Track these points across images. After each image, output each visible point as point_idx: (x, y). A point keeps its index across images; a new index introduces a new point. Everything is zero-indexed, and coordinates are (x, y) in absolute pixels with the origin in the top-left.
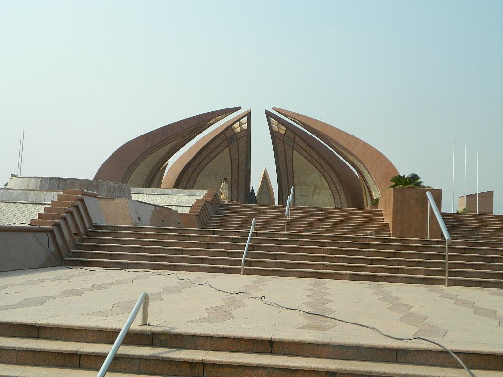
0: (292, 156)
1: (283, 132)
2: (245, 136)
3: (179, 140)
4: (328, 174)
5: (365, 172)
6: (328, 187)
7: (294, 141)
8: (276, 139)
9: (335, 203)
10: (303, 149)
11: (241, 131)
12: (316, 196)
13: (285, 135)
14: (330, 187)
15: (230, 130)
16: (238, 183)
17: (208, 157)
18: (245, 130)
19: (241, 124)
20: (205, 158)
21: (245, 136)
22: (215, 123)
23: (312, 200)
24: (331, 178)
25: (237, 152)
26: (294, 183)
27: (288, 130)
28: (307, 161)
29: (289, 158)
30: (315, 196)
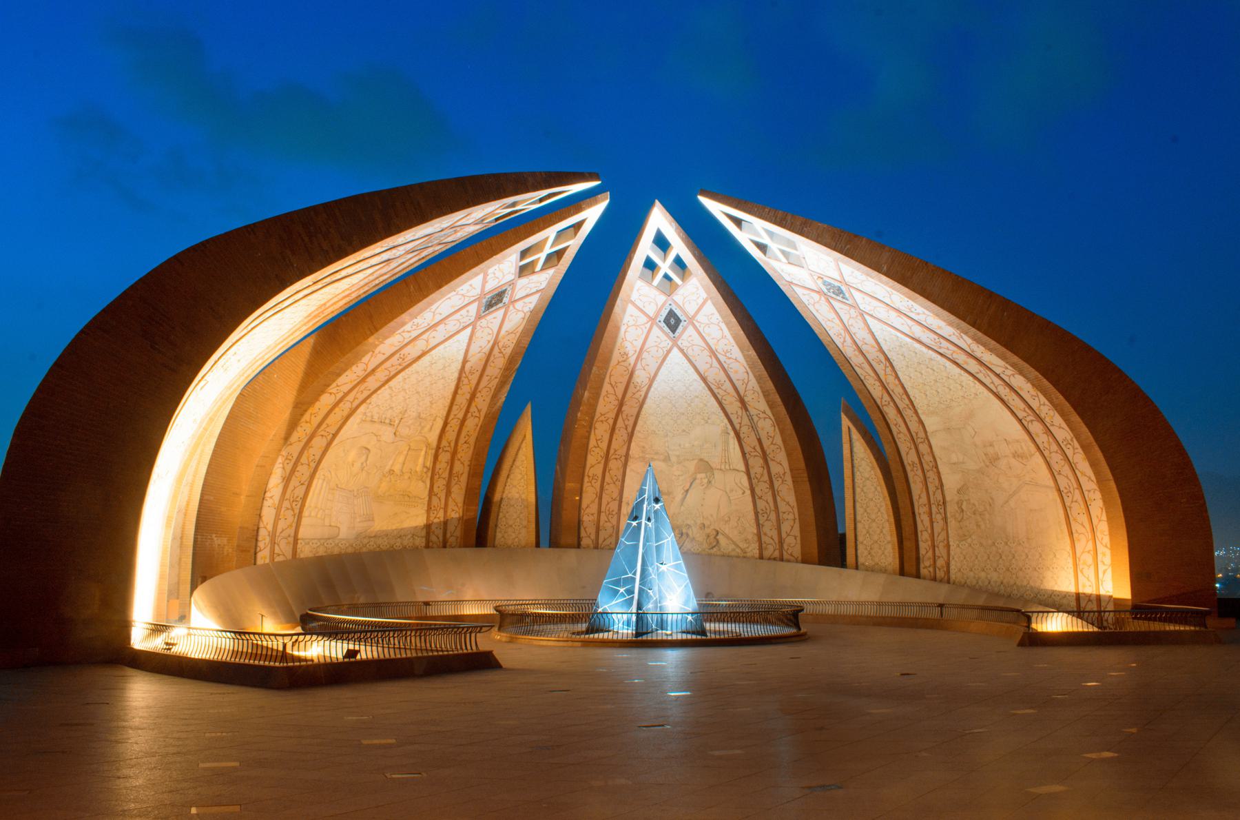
6: (742, 467)
7: (691, 320)
9: (756, 513)
14: (747, 465)
16: (454, 453)
24: (759, 440)
26: (627, 456)
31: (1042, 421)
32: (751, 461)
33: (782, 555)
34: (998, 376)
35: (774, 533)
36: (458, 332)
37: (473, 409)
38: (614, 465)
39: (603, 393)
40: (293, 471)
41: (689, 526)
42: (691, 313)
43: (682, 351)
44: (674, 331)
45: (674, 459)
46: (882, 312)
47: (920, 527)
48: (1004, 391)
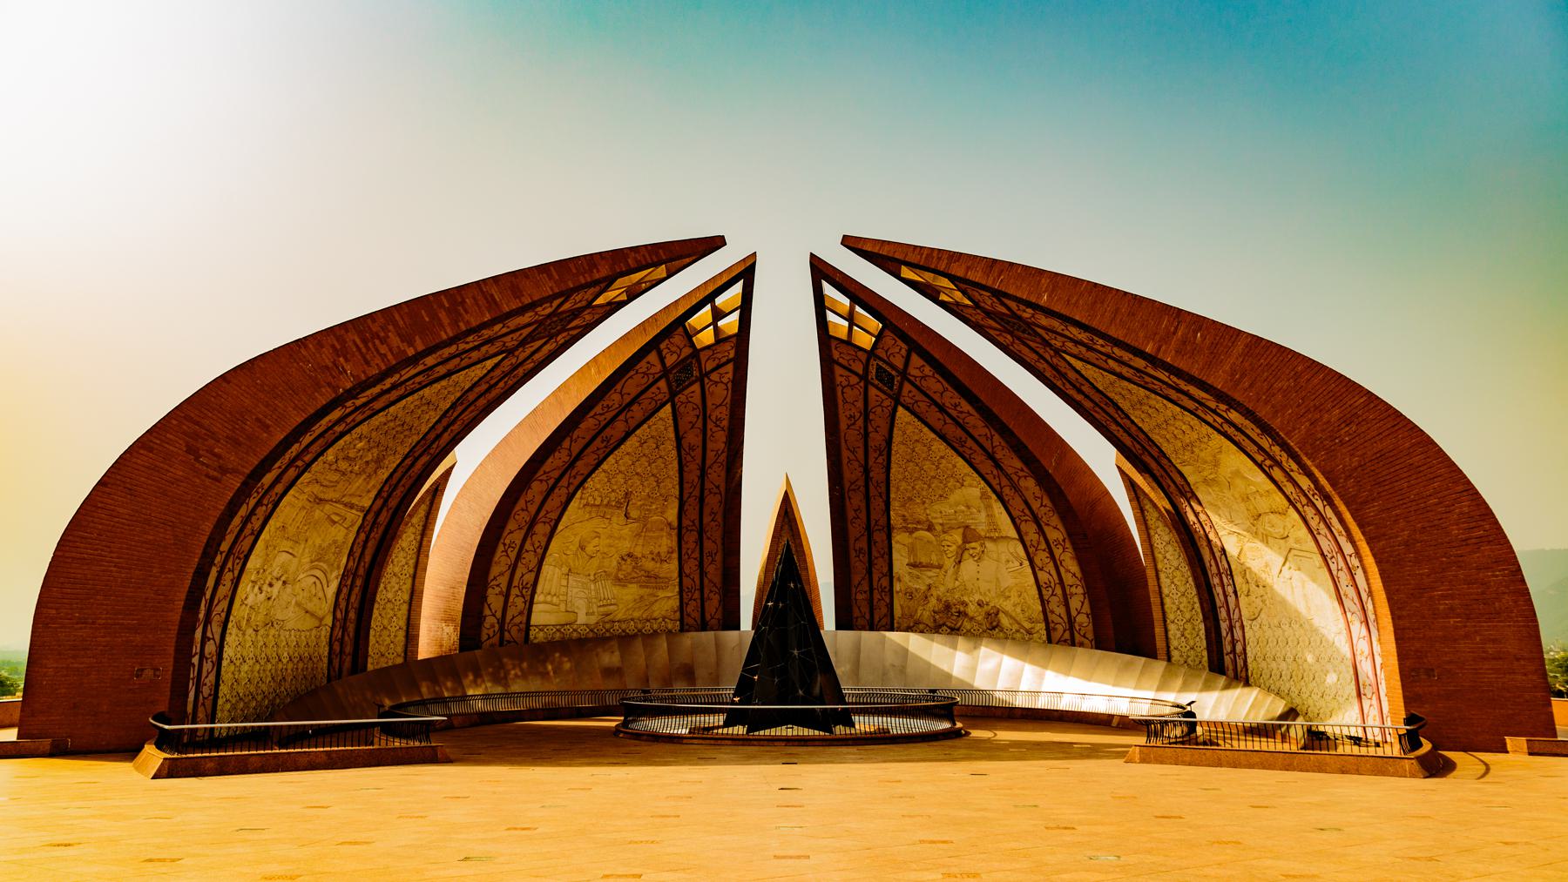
3: (489, 364)
4: (1016, 488)
6: (1014, 534)
7: (904, 374)
8: (838, 371)
10: (937, 405)
12: (969, 566)
13: (872, 353)
15: (678, 339)
16: (701, 532)
17: (598, 440)
19: (718, 314)
20: (587, 445)
24: (1026, 502)
25: (699, 424)
27: (887, 333)
28: (943, 446)
29: (876, 439)
31: (1279, 464)
32: (1023, 527)
33: (1072, 635)
34: (1214, 411)
35: (1061, 610)
36: (657, 410)
37: (708, 485)
38: (879, 537)
39: (845, 461)
41: (965, 604)
43: (907, 408)
44: (891, 388)
45: (939, 528)
46: (1075, 350)
47: (1218, 604)
48: (1231, 431)
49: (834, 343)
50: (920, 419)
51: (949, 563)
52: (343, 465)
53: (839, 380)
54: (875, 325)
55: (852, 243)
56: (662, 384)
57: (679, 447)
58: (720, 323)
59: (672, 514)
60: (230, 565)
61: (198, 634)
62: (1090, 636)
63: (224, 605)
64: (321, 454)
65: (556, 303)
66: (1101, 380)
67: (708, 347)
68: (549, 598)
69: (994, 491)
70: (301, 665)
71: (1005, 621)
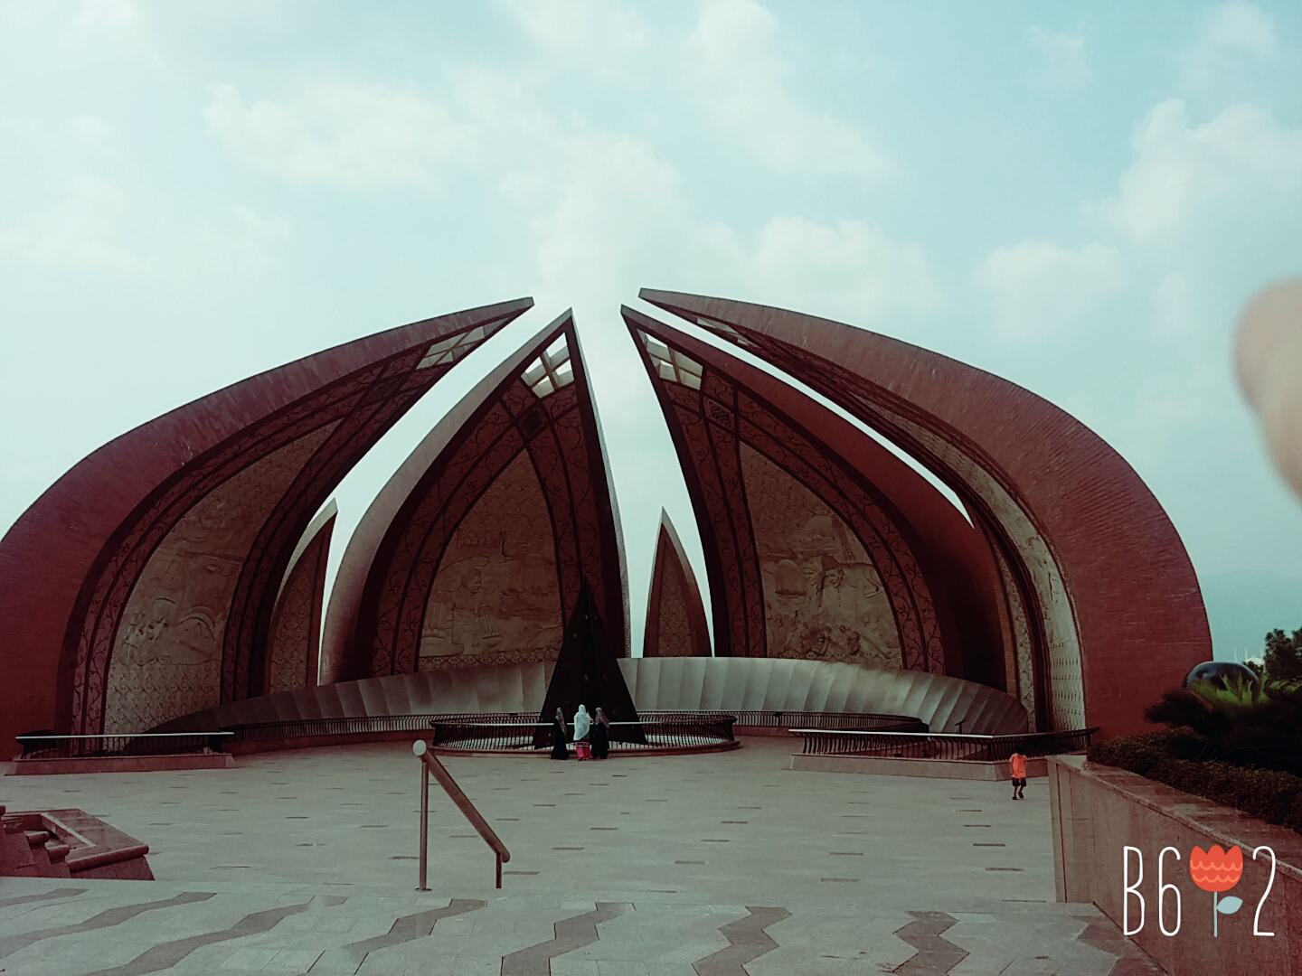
0: (739, 466)
1: (694, 382)
2: (573, 408)
3: (330, 428)
5: (997, 495)
7: (735, 409)
9: (895, 612)
10: (773, 438)
11: (558, 390)
18: (570, 384)
19: (549, 369)
20: (456, 490)
21: (573, 408)
22: (447, 367)
23: (820, 606)
30: (824, 591)
33: (926, 660)
40: (404, 596)
41: (830, 630)
42: (732, 404)
43: (747, 443)
45: (800, 556)
49: (667, 385)
50: (762, 453)
51: (813, 590)
52: (209, 523)
53: (681, 418)
54: (698, 368)
55: (646, 295)
56: (514, 431)
57: (543, 487)
58: (560, 371)
59: (549, 551)
60: (107, 612)
61: (81, 669)
62: (941, 660)
63: (107, 644)
64: (182, 515)
65: (377, 371)
66: (887, 414)
67: (550, 396)
68: (436, 631)
69: (844, 519)
70: (191, 693)
71: (865, 646)
